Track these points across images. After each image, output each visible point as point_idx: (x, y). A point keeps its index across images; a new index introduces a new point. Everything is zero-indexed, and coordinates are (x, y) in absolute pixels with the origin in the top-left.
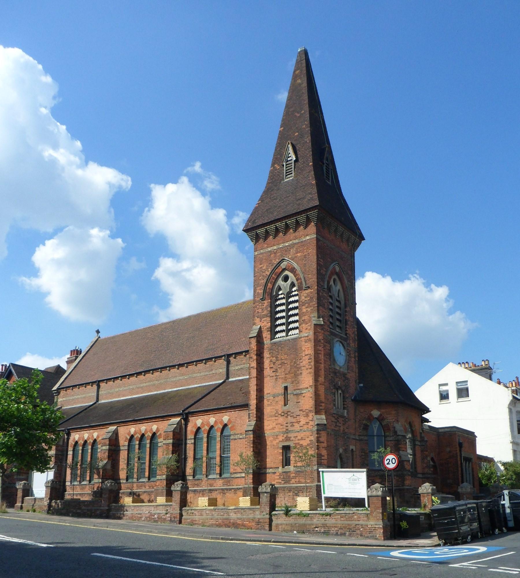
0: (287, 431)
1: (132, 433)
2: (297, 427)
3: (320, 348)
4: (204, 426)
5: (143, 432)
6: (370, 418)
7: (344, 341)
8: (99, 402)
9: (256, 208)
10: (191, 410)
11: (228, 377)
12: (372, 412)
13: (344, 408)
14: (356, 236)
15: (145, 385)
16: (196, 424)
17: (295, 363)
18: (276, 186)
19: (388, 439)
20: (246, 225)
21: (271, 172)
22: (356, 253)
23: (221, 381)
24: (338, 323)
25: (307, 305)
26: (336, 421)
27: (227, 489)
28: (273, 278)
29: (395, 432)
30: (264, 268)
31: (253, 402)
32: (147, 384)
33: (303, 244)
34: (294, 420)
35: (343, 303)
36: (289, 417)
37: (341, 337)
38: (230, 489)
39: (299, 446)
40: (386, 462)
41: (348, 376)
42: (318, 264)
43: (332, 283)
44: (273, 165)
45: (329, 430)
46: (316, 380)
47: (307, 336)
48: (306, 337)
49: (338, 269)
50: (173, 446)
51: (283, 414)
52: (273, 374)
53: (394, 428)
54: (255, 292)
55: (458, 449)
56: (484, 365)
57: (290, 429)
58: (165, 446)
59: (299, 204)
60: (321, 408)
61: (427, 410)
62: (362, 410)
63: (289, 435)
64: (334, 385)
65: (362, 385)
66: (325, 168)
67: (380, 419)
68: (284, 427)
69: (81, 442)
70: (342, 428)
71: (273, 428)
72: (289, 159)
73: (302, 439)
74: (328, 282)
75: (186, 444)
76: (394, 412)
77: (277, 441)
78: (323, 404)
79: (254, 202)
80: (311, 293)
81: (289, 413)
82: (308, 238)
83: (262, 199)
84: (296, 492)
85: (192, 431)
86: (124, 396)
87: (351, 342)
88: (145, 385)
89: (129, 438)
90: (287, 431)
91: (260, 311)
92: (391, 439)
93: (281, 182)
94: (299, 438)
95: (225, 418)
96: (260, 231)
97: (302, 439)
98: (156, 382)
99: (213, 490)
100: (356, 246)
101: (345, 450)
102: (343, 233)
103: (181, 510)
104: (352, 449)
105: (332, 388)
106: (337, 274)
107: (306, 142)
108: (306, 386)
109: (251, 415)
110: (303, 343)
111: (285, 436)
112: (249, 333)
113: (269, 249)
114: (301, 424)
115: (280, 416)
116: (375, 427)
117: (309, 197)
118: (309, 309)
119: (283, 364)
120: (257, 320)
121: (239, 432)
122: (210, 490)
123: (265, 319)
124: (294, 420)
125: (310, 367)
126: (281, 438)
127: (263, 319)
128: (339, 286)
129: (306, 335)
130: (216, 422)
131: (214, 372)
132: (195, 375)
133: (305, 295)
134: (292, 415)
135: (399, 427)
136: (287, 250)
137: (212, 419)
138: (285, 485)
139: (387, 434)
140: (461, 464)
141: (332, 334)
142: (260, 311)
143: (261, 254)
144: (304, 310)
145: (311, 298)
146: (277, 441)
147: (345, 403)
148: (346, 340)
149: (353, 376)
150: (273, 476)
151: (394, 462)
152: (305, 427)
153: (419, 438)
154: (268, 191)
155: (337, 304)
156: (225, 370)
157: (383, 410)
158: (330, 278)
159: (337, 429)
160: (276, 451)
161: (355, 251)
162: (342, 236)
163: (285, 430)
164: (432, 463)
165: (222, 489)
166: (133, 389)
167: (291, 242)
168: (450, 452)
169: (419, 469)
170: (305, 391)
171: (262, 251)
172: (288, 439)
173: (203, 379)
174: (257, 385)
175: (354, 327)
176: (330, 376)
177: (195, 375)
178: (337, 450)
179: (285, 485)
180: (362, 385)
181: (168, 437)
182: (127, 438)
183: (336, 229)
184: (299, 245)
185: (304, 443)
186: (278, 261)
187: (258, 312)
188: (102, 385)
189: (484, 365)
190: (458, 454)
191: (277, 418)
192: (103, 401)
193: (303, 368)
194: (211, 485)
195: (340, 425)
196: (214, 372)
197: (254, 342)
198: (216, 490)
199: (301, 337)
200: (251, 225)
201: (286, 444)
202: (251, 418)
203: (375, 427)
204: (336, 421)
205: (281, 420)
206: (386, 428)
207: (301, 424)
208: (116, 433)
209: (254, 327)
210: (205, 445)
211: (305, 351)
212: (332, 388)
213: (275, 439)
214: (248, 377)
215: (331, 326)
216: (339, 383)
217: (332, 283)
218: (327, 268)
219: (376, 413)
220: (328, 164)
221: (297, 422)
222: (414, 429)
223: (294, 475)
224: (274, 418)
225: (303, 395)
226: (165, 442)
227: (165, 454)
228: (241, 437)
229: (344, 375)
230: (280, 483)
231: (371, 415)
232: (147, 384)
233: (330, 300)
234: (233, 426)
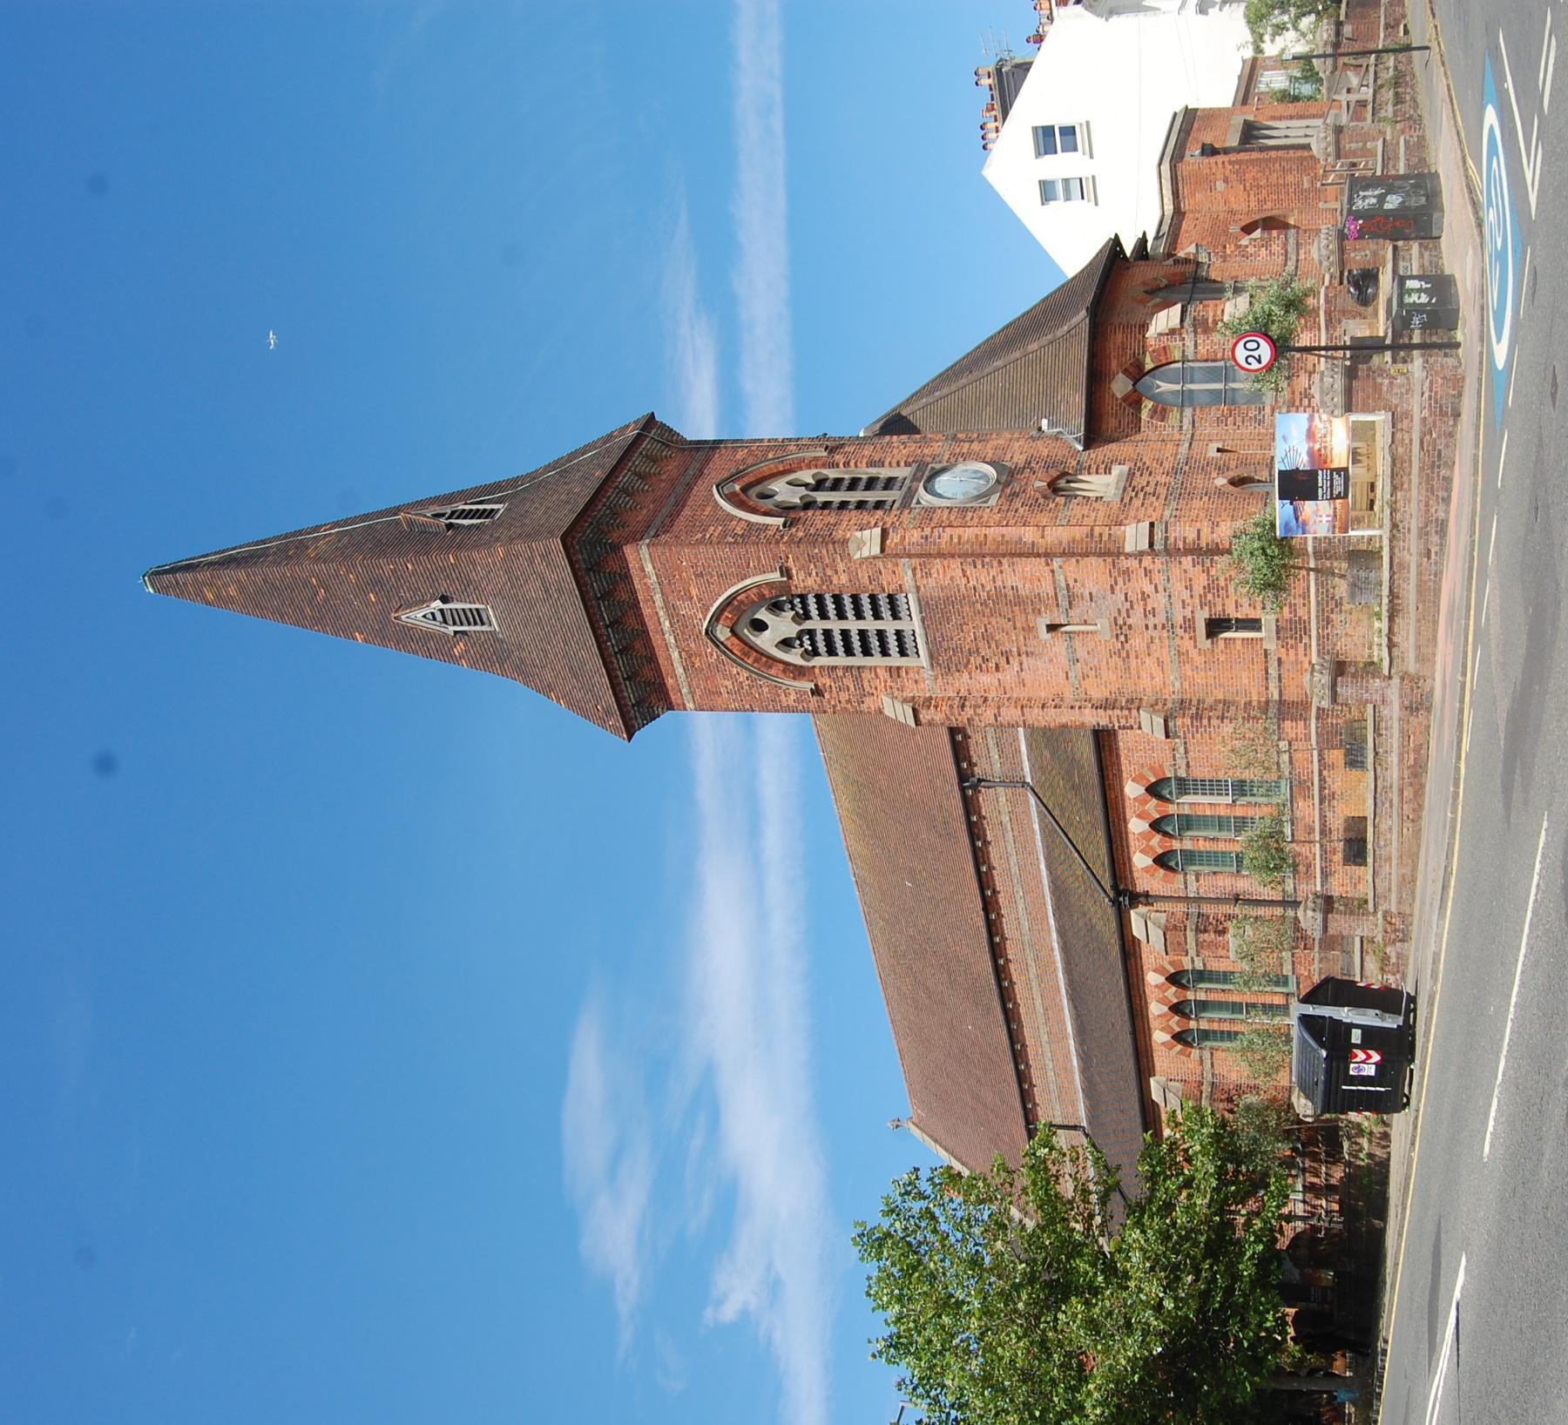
0: (1168, 625)
1: (1168, 1037)
2: (1159, 601)
3: (946, 537)
4: (1152, 848)
5: (1166, 1009)
8: (1084, 1124)
9: (570, 705)
10: (1107, 882)
11: (1024, 784)
12: (1119, 396)
13: (1108, 471)
15: (1038, 1002)
16: (1146, 870)
17: (984, 604)
18: (510, 653)
19: (1190, 353)
20: (615, 730)
21: (473, 665)
22: (690, 436)
23: (1032, 800)
25: (829, 572)
26: (1141, 495)
27: (1322, 789)
28: (756, 661)
29: (1172, 332)
30: (729, 683)
32: (1036, 994)
33: (667, 579)
34: (1139, 609)
36: (1130, 621)
38: (1322, 780)
39: (1210, 597)
40: (1255, 365)
44: (454, 659)
45: (1167, 513)
47: (914, 570)
48: (914, 575)
50: (1205, 931)
51: (1122, 638)
52: (1015, 663)
53: (1160, 334)
54: (794, 710)
56: (990, 81)
57: (1160, 619)
58: (1205, 952)
59: (558, 590)
60: (1105, 538)
61: (1116, 242)
62: (1113, 423)
63: (1178, 620)
64: (1045, 497)
65: (1044, 423)
66: (466, 522)
68: (1156, 634)
70: (1163, 479)
71: (1160, 663)
72: (439, 616)
73: (1189, 588)
75: (1199, 900)
76: (1119, 336)
77: (1194, 653)
78: (1097, 530)
79: (554, 711)
80: (796, 559)
81: (1120, 622)
82: (649, 568)
83: (547, 690)
84: (1332, 604)
85: (1164, 879)
86: (1067, 1055)
87: (926, 451)
88: (1038, 1002)
89: (1179, 1047)
90: (1168, 625)
91: (844, 696)
92: (1190, 343)
93: (501, 641)
94: (1186, 595)
95: (1132, 790)
96: (630, 696)
97: (1189, 588)
98: (1033, 972)
99: (1323, 824)
100: (669, 438)
101: (1221, 470)
102: (635, 473)
104: (1219, 450)
105: (1052, 505)
106: (744, 490)
107: (394, 571)
108: (1048, 575)
109: (1123, 722)
110: (931, 582)
111: (1180, 632)
112: (904, 726)
113: (679, 670)
114: (1149, 589)
115: (1127, 646)
117: (540, 566)
118: (841, 566)
119: (988, 637)
120: (869, 704)
121: (1169, 754)
122: (1322, 832)
123: (866, 684)
124: (1139, 609)
125: (995, 564)
126: (1187, 644)
127: (867, 689)
129: (910, 573)
130: (1140, 816)
131: (1005, 819)
132: (1015, 870)
133: (802, 575)
134: (1124, 614)
138: (1314, 633)
139: (1177, 355)
142: (844, 696)
143: (692, 693)
144: (844, 579)
145: (811, 559)
146: (1194, 653)
147: (1094, 467)
150: (1285, 666)
151: (1254, 345)
152: (1159, 579)
154: (523, 672)
156: (1000, 790)
157: (1114, 364)
159: (1162, 491)
160: (1222, 658)
161: (683, 441)
162: (642, 477)
163: (1165, 634)
164: (1257, 234)
165: (1321, 802)
166: (1049, 1033)
167: (661, 613)
168: (1226, 180)
170: (1062, 578)
171: (684, 691)
172: (1189, 625)
173: (1025, 847)
175: (889, 444)
176: (1021, 510)
177: (1015, 870)
178: (1219, 492)
179: (1314, 633)
180: (1044, 423)
181: (1179, 944)
182: (1180, 1053)
183: (625, 491)
184: (667, 590)
185: (1201, 581)
186: (710, 648)
187: (849, 701)
189: (990, 81)
190: (1233, 157)
191: (1132, 655)
192: (1082, 1113)
193: (999, 583)
194: (1311, 831)
195: (1152, 484)
196: (1005, 819)
198: (1323, 817)
199: (918, 588)
200: (616, 720)
202: (1131, 721)
204: (1141, 495)
205: (1137, 642)
207: (1149, 589)
209: (889, 712)
211: (952, 579)
212: (1052, 505)
213: (1189, 661)
214: (1021, 730)
216: (1038, 484)
217: (768, 504)
220: (453, 513)
221: (1144, 599)
222: (1165, 282)
223: (1286, 609)
224: (1133, 662)
225: (1072, 584)
226: (1192, 952)
227: (1221, 952)
228: (1182, 750)
230: (1307, 647)
231: (1125, 399)
232: (1036, 994)
234: (1152, 769)
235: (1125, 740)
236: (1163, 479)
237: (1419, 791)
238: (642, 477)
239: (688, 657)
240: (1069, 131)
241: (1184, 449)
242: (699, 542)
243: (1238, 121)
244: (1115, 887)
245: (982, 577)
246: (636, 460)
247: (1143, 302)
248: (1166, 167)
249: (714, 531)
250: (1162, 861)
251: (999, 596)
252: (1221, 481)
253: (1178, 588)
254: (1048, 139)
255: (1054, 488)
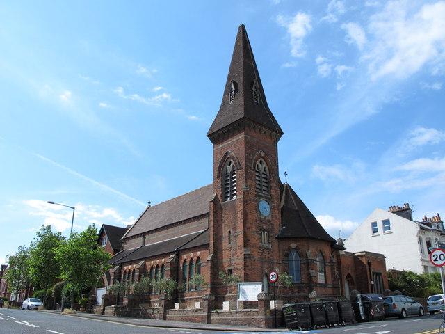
2: (235, 257)
6: (290, 249)
7: (268, 200)
14: (276, 131)
22: (279, 143)
24: (264, 188)
31: (212, 242)
33: (238, 142)
35: (268, 175)
37: (266, 198)
41: (273, 222)
42: (246, 152)
43: (258, 163)
46: (244, 226)
49: (263, 154)
55: (367, 267)
67: (297, 249)
69: (128, 271)
70: (267, 257)
74: (255, 164)
83: (217, 117)
90: (231, 260)
95: (198, 253)
100: (277, 139)
103: (165, 311)
116: (294, 255)
128: (264, 165)
135: (310, 254)
136: (229, 146)
137: (192, 254)
140: (371, 277)
141: (258, 195)
148: (270, 199)
149: (277, 222)
153: (328, 261)
155: (263, 176)
158: (256, 160)
161: (277, 141)
162: (265, 133)
169: (329, 282)
172: (231, 265)
173: (197, 229)
174: (214, 231)
188: (147, 237)
190: (368, 269)
197: (212, 203)
201: (230, 268)
203: (294, 255)
206: (301, 255)
208: (144, 265)
210: (188, 270)
215: (258, 190)
217: (258, 163)
218: (254, 155)
219: (293, 245)
229: (269, 221)
233: (257, 174)
235: (208, 251)
236: (267, 257)
237: (187, 321)
238: (265, 133)
239: (223, 148)
240: (389, 228)
241: (276, 261)
242: (246, 148)
243: (381, 272)
244: (179, 251)
245: (240, 215)
246: (269, 132)
247: (317, 250)
248: (364, 253)
249: (249, 151)
250: (185, 261)
251: (236, 220)
252: (266, 271)
253: (237, 262)
254: (386, 222)
255: (263, 230)
